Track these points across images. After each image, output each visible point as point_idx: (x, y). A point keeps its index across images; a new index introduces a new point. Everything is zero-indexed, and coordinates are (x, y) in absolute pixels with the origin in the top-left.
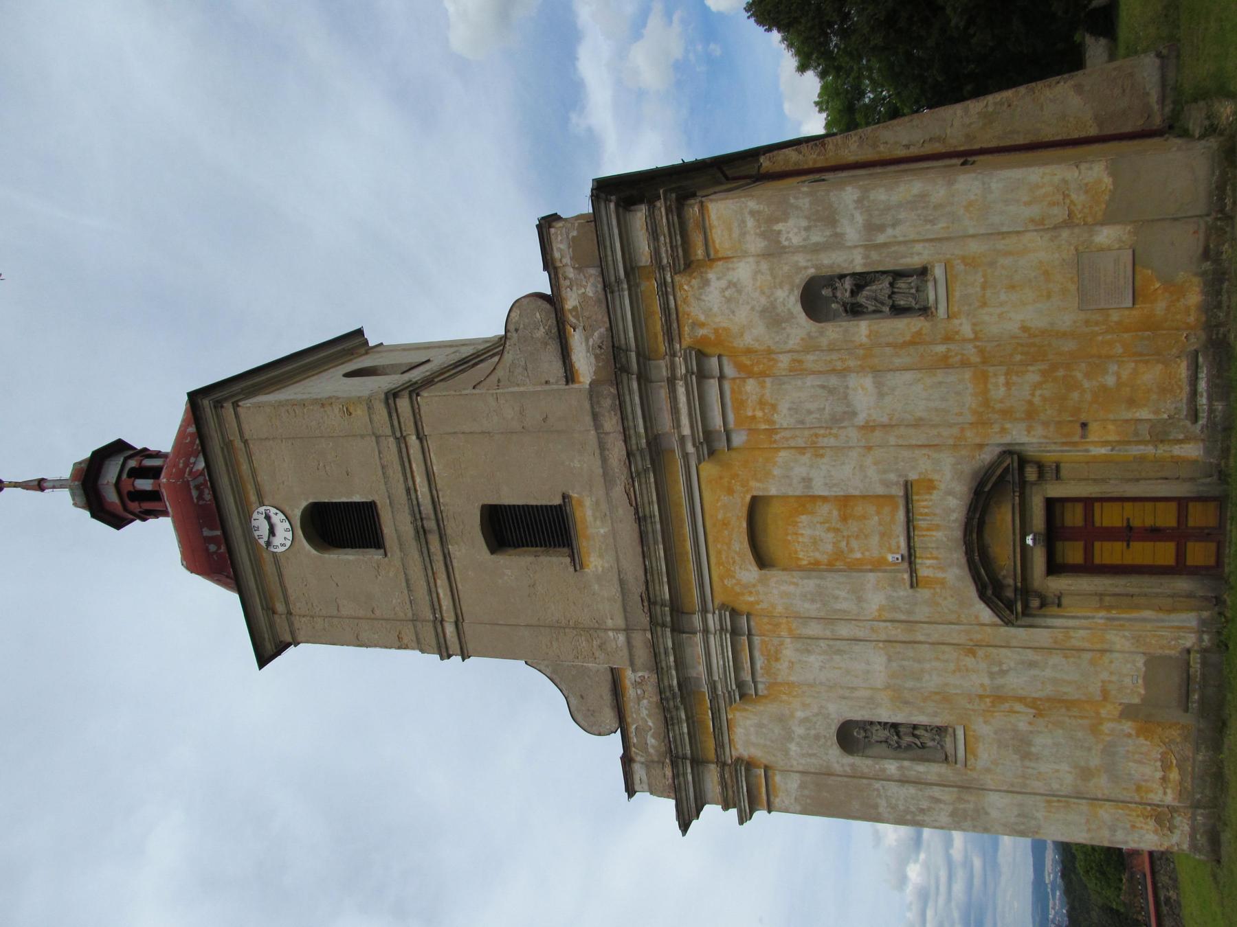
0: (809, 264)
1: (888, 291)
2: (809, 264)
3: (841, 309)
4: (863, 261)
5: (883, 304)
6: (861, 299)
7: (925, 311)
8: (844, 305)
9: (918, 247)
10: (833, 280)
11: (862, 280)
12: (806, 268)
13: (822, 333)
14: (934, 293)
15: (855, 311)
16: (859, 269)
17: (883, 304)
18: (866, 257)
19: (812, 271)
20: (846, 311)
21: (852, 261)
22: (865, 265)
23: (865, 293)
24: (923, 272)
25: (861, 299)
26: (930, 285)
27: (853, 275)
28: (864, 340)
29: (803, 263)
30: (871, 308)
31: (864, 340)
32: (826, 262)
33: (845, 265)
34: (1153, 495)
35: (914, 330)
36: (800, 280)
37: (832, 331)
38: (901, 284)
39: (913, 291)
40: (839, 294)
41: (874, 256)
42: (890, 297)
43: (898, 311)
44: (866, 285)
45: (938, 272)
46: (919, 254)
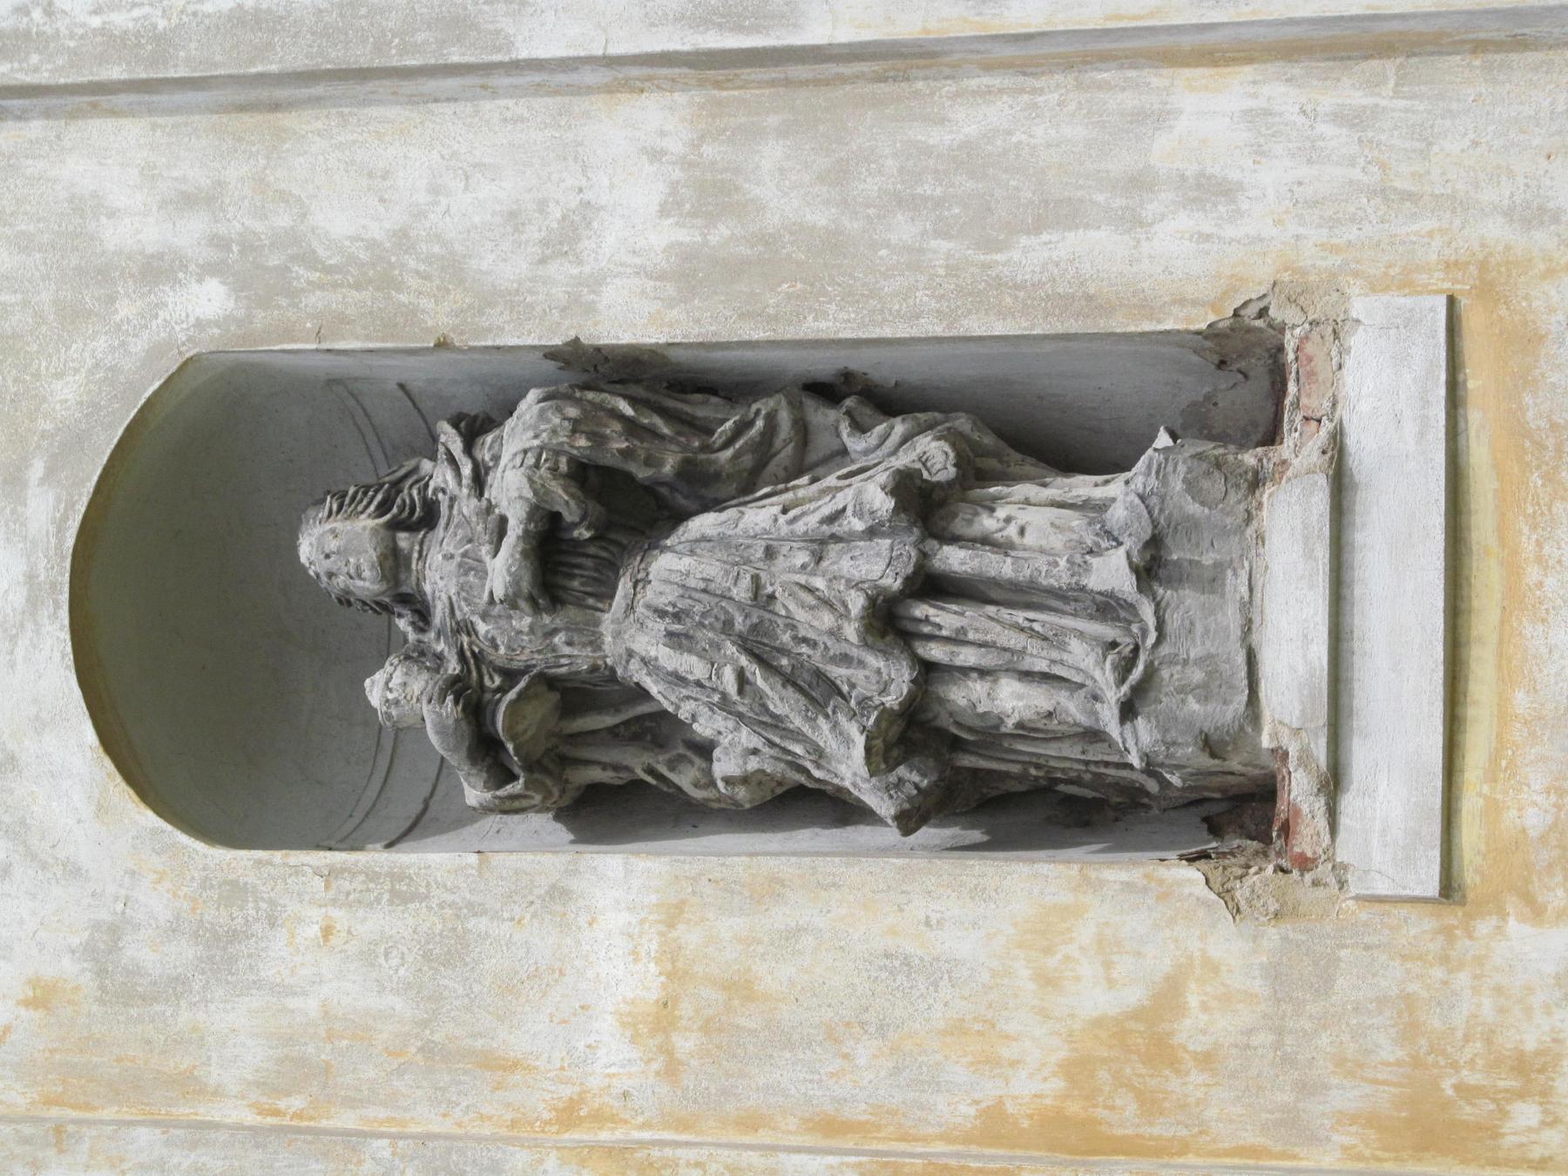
0: (189, 233)
1: (878, 565)
2: (189, 233)
3: (437, 719)
4: (663, 237)
5: (820, 691)
6: (641, 631)
7: (1232, 811)
8: (469, 695)
9: (1206, 114)
10: (370, 431)
11: (654, 438)
12: (157, 270)
13: (223, 950)
14: (1306, 613)
15: (592, 764)
16: (630, 319)
17: (820, 691)
18: (707, 194)
19: (201, 312)
20: (485, 749)
21: (565, 239)
22: (687, 274)
23: (676, 566)
24: (1241, 384)
25: (641, 631)
26: (1291, 515)
27: (591, 371)
28: (614, 1061)
29: (136, 227)
30: (736, 754)
31: (614, 1061)
32: (342, 221)
33: (505, 266)
34: (1438, 621)
35: (1095, 997)
36: (86, 390)
37: (330, 931)
38: (1032, 523)
39: (1112, 572)
40: (438, 575)
41: (782, 179)
42: (887, 621)
43: (985, 791)
44: (704, 488)
45: (1377, 390)
46: (1209, 191)
